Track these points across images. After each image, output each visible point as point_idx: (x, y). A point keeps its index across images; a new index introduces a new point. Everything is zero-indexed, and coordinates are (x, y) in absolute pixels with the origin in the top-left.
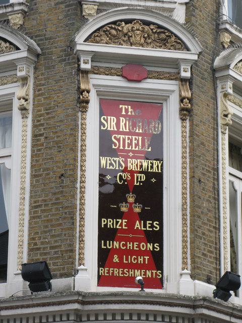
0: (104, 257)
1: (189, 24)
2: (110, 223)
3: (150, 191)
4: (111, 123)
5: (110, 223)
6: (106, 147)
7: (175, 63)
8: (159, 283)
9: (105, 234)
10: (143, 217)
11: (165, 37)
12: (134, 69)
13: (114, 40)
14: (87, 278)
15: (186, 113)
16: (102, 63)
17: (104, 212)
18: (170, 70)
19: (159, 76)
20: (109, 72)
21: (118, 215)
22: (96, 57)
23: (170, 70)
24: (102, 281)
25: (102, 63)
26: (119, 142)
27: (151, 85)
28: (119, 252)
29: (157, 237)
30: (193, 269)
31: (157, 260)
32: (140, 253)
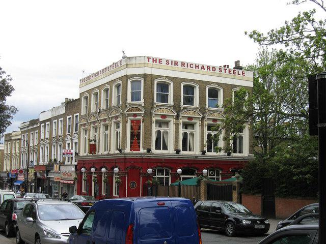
0: (131, 146)
6: (132, 128)
7: (141, 114)
9: (131, 143)
11: (139, 110)
12: (135, 115)
13: (131, 111)
14: (128, 150)
16: (129, 115)
17: (131, 139)
18: (140, 115)
19: (139, 116)
22: (128, 114)
23: (140, 115)
24: (131, 150)
25: (129, 115)
27: (138, 118)
29: (139, 143)
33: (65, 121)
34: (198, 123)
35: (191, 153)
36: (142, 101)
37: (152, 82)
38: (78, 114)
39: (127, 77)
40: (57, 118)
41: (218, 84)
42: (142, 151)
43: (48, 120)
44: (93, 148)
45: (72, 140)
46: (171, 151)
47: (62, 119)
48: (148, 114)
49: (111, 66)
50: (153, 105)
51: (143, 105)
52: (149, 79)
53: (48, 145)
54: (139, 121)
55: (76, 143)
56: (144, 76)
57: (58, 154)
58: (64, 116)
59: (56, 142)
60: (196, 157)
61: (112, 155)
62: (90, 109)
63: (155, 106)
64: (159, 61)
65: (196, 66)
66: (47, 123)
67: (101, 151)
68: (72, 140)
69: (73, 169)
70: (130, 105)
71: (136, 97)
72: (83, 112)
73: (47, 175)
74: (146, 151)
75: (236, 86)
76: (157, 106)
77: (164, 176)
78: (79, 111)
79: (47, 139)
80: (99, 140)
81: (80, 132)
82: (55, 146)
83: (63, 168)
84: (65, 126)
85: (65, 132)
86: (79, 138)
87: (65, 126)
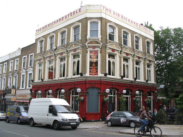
1: (101, 41)
2: (91, 67)
3: (96, 63)
4: (91, 54)
5: (91, 67)
6: (91, 57)
7: (99, 46)
8: (97, 75)
9: (90, 69)
10: (95, 66)
11: (98, 43)
12: (94, 47)
13: (91, 44)
14: (88, 74)
15: (101, 52)
16: (89, 47)
17: (90, 66)
18: (98, 47)
19: (97, 48)
20: (90, 48)
21: (92, 66)
22: (88, 46)
23: (98, 47)
24: (90, 75)
25: (89, 47)
26: (92, 57)
28: (92, 71)
29: (97, 69)
30: (102, 72)
31: (97, 72)
32: (94, 71)
33: (21, 60)
34: (131, 59)
35: (127, 79)
36: (100, 36)
37: (106, 24)
38: (33, 54)
39: (87, 19)
40: (14, 59)
41: (140, 34)
42: (100, 75)
43: (5, 62)
44: (51, 75)
45: (27, 72)
46: (117, 76)
47: (18, 59)
48: (104, 47)
49: (68, 15)
50: (107, 41)
51: (100, 40)
52: (104, 21)
53: (5, 78)
54: (96, 52)
55: (30, 74)
56: (101, 19)
57: (12, 82)
58: (20, 57)
59: (13, 75)
60: (132, 82)
61: (70, 79)
62: (45, 48)
63: (108, 42)
64: (110, 11)
65: (129, 20)
66: (5, 63)
67: (57, 77)
68: (27, 72)
69: (30, 92)
70: (89, 39)
71: (94, 32)
72: (38, 51)
73: (4, 97)
74: (103, 75)
75: (147, 38)
76: (109, 42)
77: (112, 96)
78: (34, 51)
79: (5, 73)
80: (55, 69)
81: (35, 65)
82: (10, 78)
83: (18, 92)
84: (20, 64)
85: (20, 68)
86: (34, 71)
87: (20, 64)
